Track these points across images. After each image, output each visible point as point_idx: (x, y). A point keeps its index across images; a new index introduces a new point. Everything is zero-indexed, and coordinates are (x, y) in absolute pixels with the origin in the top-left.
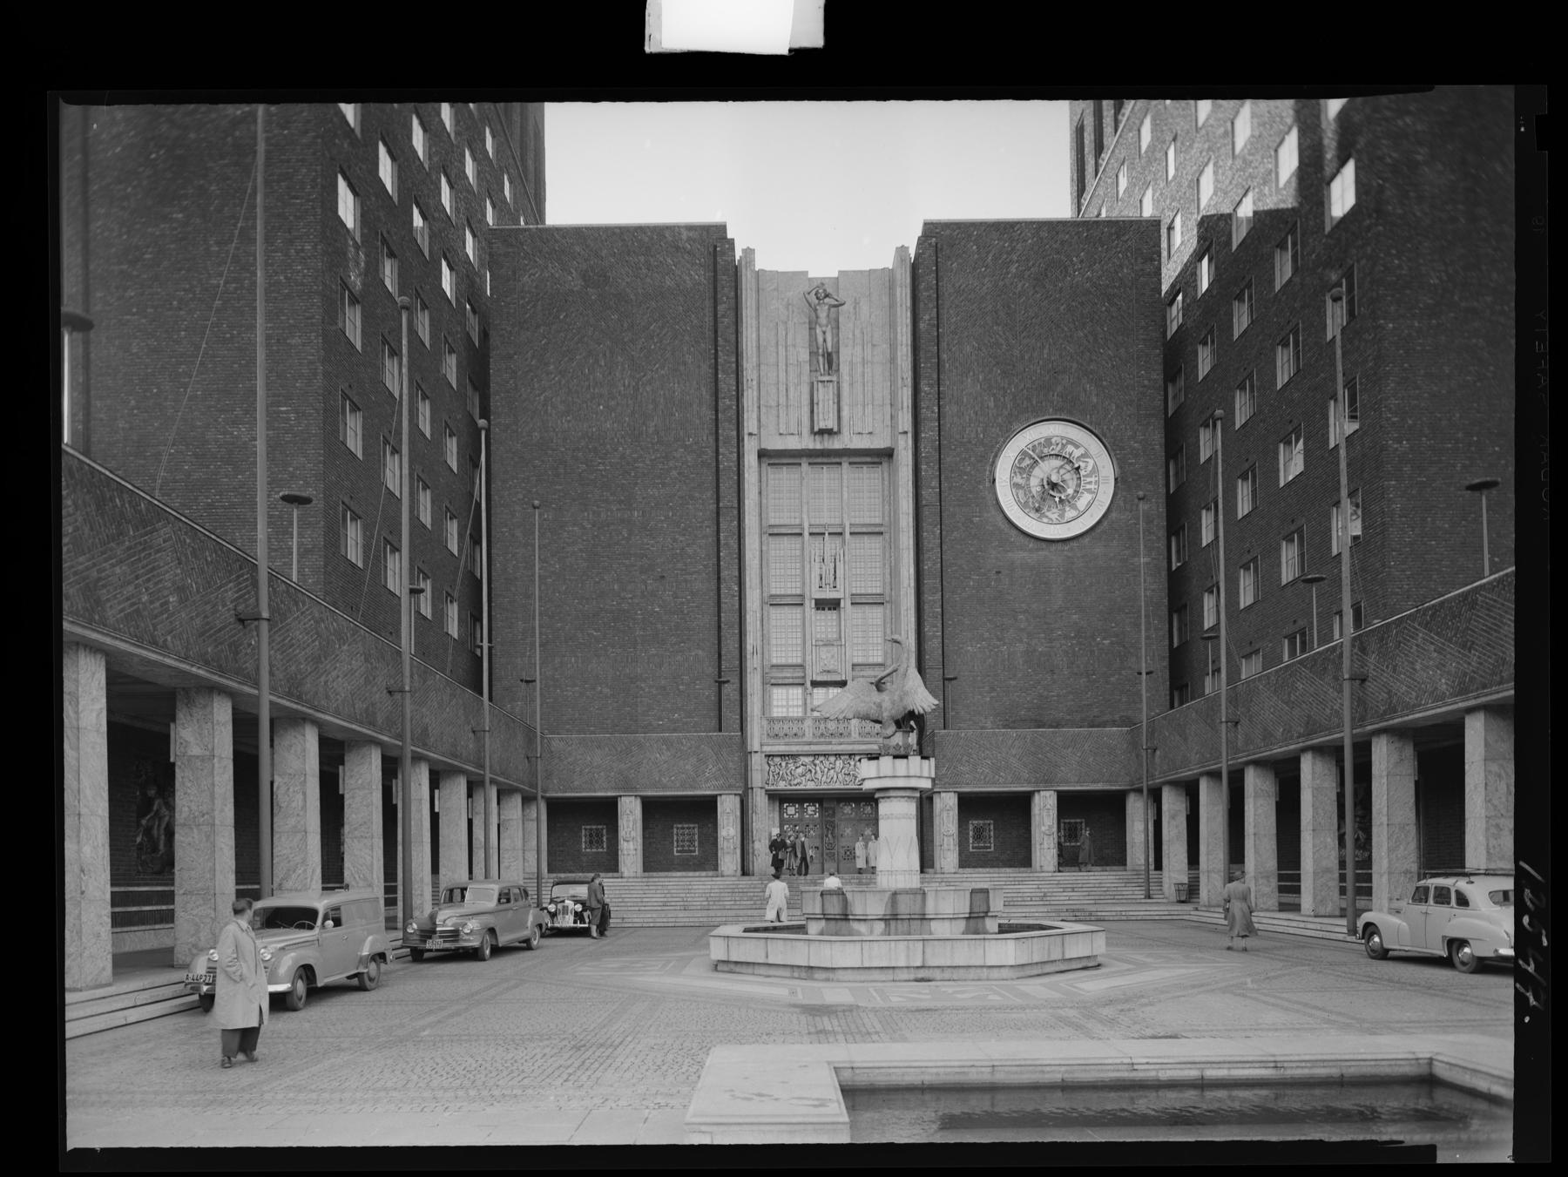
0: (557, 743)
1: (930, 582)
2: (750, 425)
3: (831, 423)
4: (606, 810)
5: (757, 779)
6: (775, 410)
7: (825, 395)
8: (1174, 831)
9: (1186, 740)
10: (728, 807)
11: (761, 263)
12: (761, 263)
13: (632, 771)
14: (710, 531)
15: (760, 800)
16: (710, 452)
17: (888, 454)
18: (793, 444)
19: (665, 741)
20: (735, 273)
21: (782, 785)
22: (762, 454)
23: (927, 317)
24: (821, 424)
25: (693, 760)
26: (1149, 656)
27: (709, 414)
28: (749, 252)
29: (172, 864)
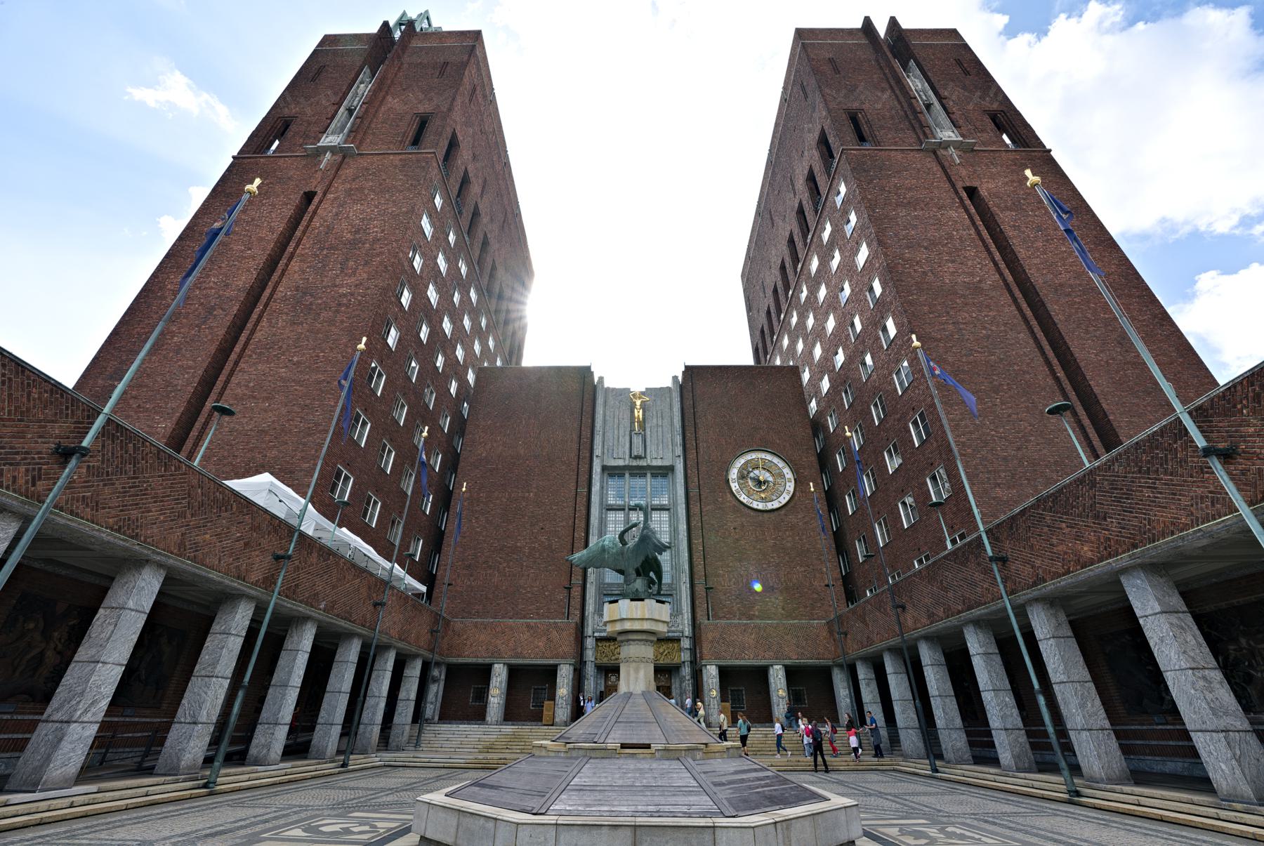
0: (458, 624)
1: (696, 533)
2: (598, 451)
3: (641, 452)
4: (484, 672)
5: (590, 655)
6: (611, 447)
7: (637, 441)
8: (869, 694)
9: (867, 625)
10: (565, 675)
11: (606, 385)
12: (606, 385)
13: (500, 646)
14: (572, 504)
15: (590, 670)
16: (575, 463)
17: (670, 469)
18: (621, 463)
19: (528, 626)
20: (594, 388)
21: (605, 660)
22: (604, 468)
23: (689, 403)
24: (635, 453)
25: (544, 639)
26: (830, 571)
27: (575, 446)
28: (601, 379)
29: (47, 698)
